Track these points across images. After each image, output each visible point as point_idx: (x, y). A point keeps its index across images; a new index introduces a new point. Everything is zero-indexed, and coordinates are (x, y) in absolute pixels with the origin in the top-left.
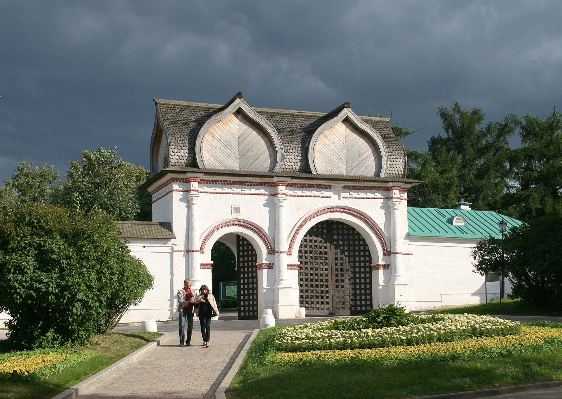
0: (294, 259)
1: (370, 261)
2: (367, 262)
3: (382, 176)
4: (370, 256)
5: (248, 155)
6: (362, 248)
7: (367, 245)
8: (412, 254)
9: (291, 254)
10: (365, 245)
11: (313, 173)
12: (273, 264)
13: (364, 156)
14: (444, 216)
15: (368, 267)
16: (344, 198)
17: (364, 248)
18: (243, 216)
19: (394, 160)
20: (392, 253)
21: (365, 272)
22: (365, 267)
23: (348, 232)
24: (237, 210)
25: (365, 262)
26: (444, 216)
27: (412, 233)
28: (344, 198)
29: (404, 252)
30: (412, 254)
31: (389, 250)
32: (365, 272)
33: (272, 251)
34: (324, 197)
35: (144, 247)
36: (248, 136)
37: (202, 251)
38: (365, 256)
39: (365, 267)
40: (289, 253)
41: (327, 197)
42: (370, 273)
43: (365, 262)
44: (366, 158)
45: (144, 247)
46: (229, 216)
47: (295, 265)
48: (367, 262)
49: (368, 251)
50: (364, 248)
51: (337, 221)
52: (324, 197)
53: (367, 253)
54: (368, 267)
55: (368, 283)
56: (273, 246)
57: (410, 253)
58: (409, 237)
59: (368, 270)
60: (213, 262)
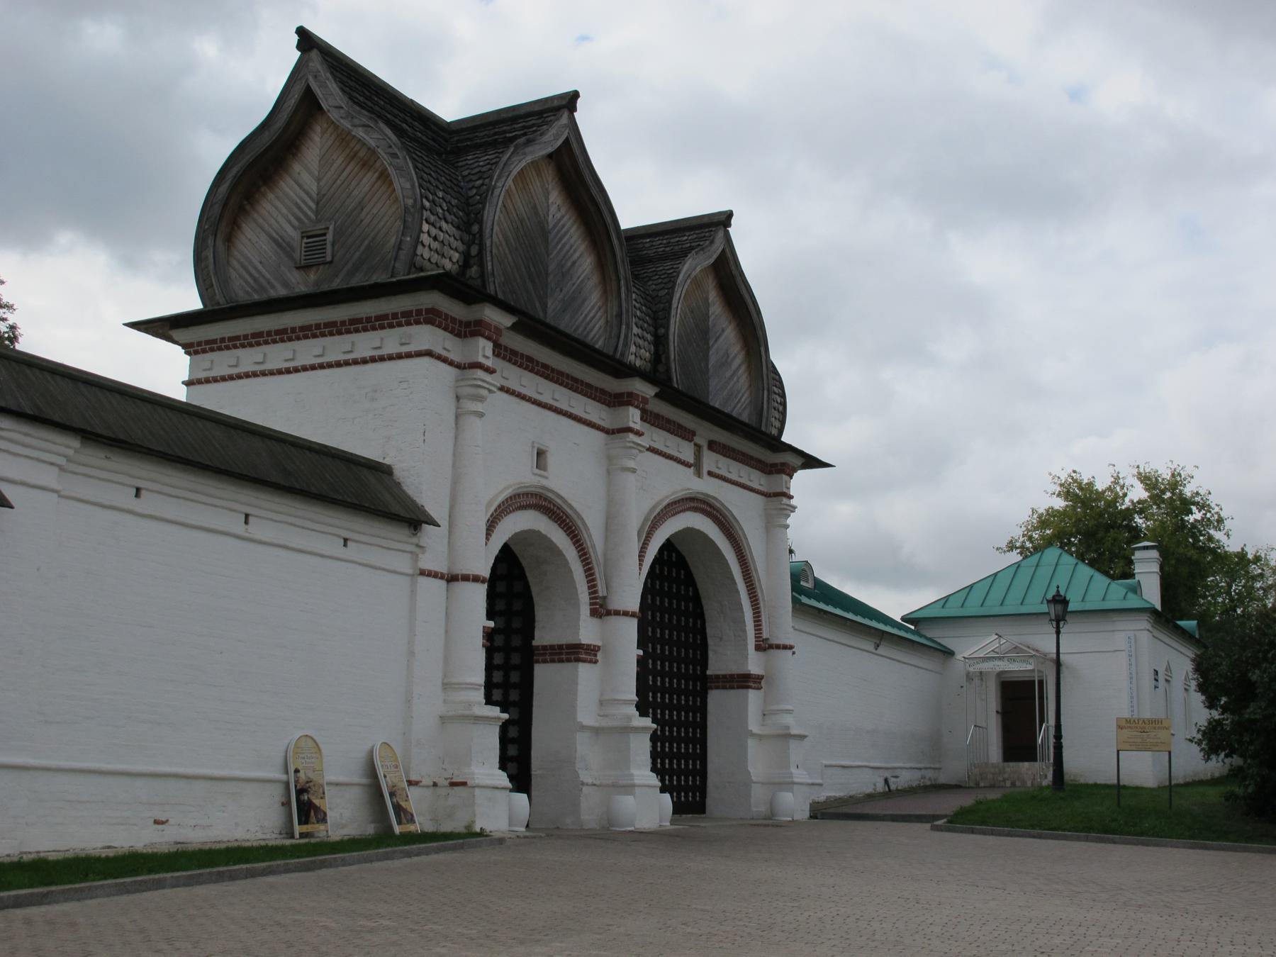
1: (705, 665)
5: (565, 290)
28: (710, 474)
33: (601, 610)
56: (602, 592)
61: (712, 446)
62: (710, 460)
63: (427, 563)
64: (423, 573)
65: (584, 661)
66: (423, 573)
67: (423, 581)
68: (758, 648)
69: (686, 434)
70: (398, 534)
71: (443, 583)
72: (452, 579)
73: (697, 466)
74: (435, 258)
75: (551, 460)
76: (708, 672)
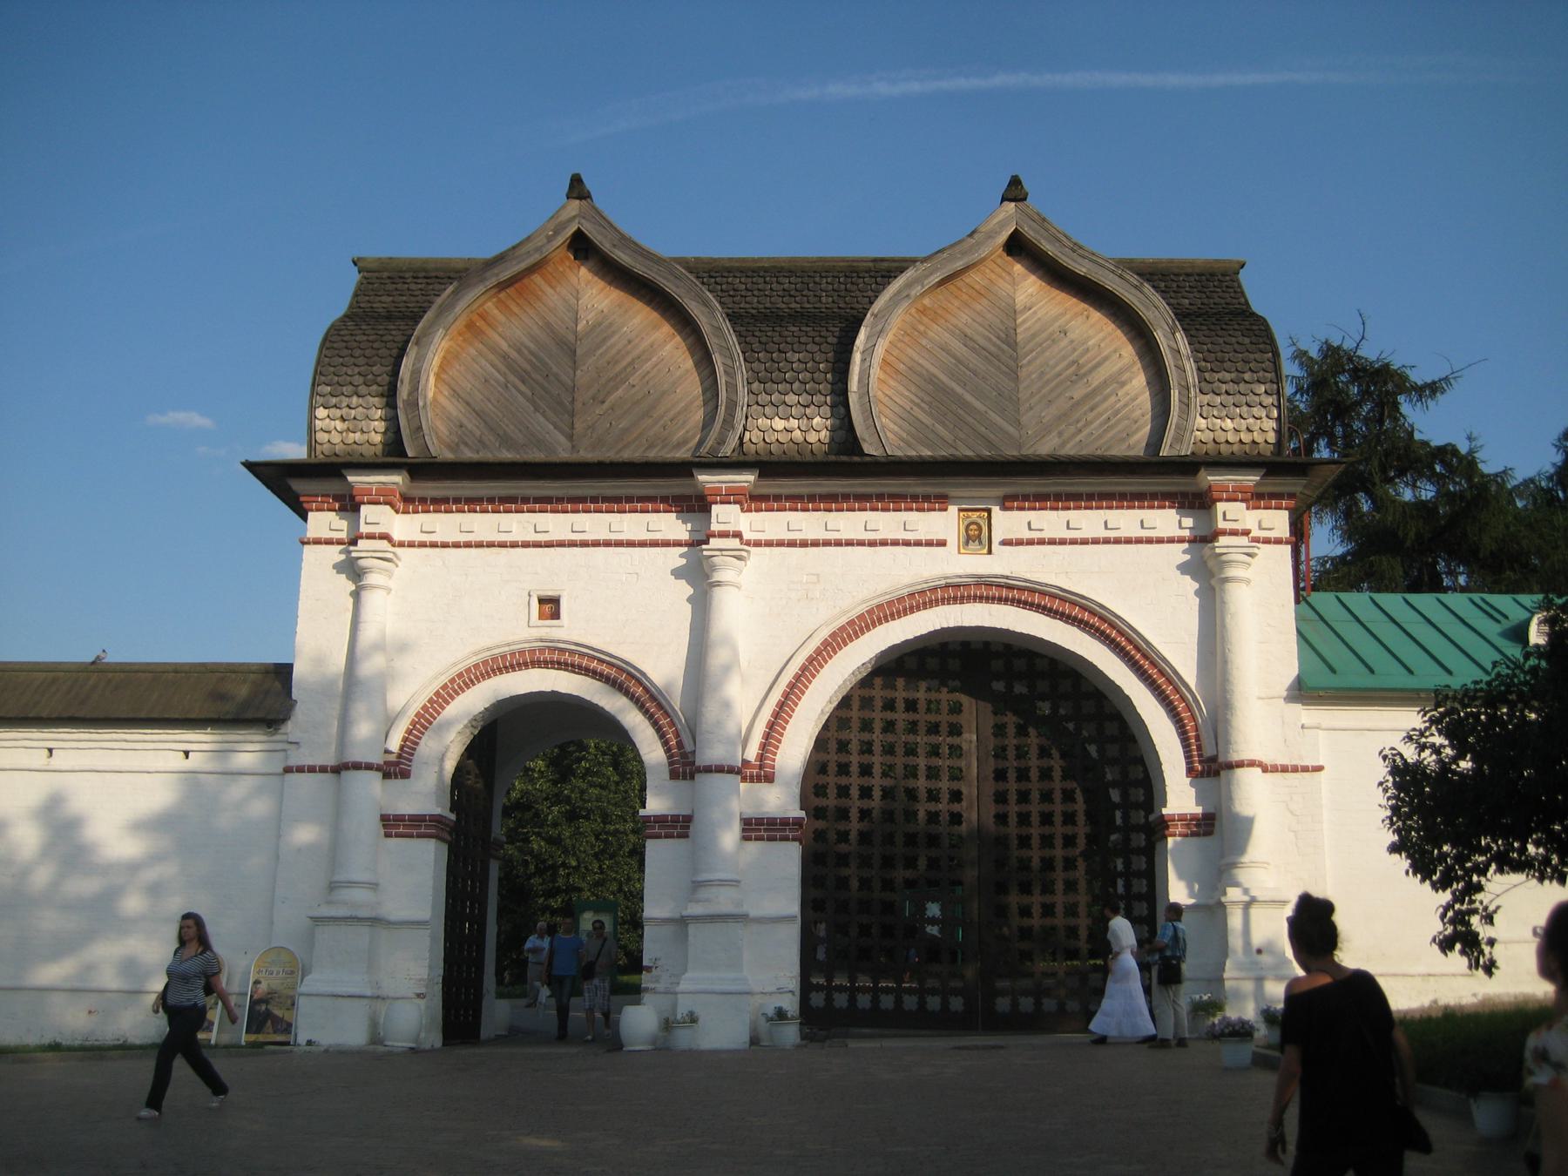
8: (1319, 769)
11: (867, 449)
12: (688, 819)
13: (1097, 378)
16: (1005, 543)
18: (570, 629)
19: (1231, 387)
24: (551, 606)
26: (1493, 614)
28: (1005, 543)
29: (1281, 760)
30: (1319, 769)
31: (1208, 752)
33: (685, 766)
34: (918, 543)
35: (187, 754)
36: (614, 333)
41: (929, 543)
44: (1105, 384)
45: (187, 754)
46: (525, 630)
47: (785, 822)
51: (1008, 647)
52: (918, 543)
56: (688, 747)
57: (1310, 763)
58: (1303, 692)
61: (1007, 503)
62: (1006, 522)
65: (658, 837)
66: (288, 770)
67: (289, 776)
71: (328, 777)
72: (337, 770)
73: (977, 537)
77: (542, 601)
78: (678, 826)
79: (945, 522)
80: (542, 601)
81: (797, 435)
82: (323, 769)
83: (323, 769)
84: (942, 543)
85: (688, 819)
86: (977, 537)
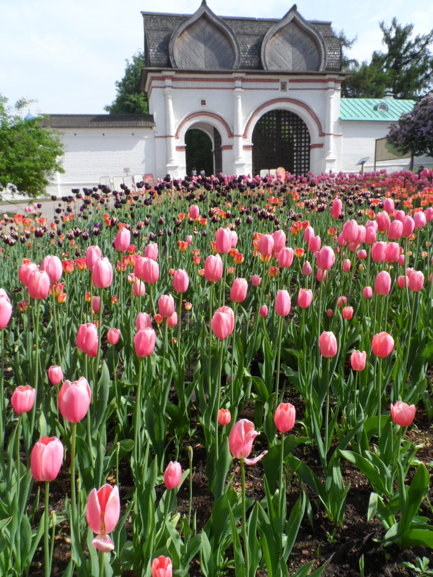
0: (249, 142)
1: (309, 142)
2: (307, 142)
3: (321, 70)
4: (309, 138)
6: (303, 131)
7: (307, 129)
9: (246, 137)
10: (306, 129)
14: (370, 104)
15: (307, 146)
17: (305, 131)
20: (236, 136)
21: (305, 151)
22: (305, 147)
23: (293, 118)
24: (203, 103)
25: (305, 142)
26: (370, 104)
27: (343, 118)
28: (290, 89)
32: (305, 151)
33: (231, 135)
37: (177, 136)
38: (305, 138)
39: (305, 147)
40: (245, 136)
42: (309, 151)
43: (305, 142)
47: (249, 146)
48: (307, 142)
49: (308, 133)
50: (305, 131)
53: (307, 136)
54: (307, 146)
55: (307, 159)
59: (307, 149)
60: (186, 145)
61: (291, 81)
62: (289, 85)
63: (157, 135)
64: (156, 137)
66: (156, 137)
67: (157, 139)
68: (320, 136)
69: (277, 81)
70: (149, 129)
71: (164, 139)
72: (166, 137)
74: (158, 62)
75: (206, 102)
76: (310, 144)
77: (202, 101)
78: (230, 147)
79: (278, 85)
80: (202, 101)
81: (250, 64)
82: (163, 137)
83: (163, 137)
84: (278, 89)
85: (232, 146)
86: (284, 88)
